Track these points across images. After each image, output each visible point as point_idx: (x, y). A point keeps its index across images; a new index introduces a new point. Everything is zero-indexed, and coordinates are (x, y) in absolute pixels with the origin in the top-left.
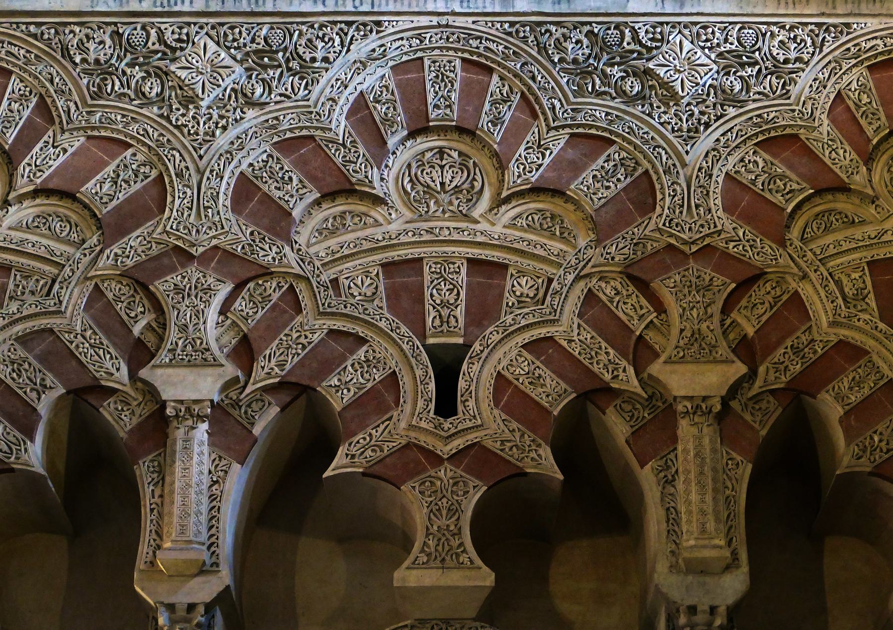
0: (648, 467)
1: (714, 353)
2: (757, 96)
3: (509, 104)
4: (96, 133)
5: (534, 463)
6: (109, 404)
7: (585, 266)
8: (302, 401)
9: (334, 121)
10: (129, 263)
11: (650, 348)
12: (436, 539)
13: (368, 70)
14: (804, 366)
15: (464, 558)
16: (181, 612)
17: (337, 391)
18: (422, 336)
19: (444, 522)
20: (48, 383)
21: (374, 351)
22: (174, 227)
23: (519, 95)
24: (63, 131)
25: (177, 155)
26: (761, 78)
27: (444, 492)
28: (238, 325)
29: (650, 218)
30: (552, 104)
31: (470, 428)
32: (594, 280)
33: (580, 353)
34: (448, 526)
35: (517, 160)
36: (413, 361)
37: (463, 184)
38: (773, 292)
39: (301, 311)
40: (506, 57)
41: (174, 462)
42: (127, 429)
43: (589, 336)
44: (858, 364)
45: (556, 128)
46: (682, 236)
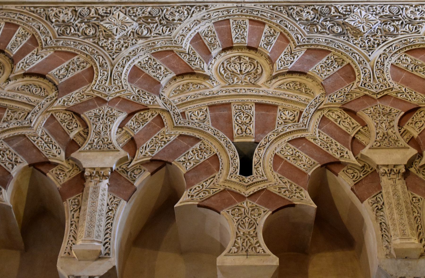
0: (366, 202)
1: (397, 144)
2: (403, 33)
3: (274, 37)
4: (59, 49)
5: (299, 199)
6: (52, 171)
7: (320, 105)
8: (163, 170)
10: (71, 104)
12: (242, 240)
13: (201, 24)
15: (259, 249)
18: (232, 138)
19: (246, 230)
20: (19, 160)
21: (204, 145)
22: (97, 88)
23: (279, 34)
24: (42, 49)
25: (101, 58)
26: (404, 26)
27: (246, 214)
28: (128, 133)
29: (353, 84)
31: (260, 181)
32: (326, 112)
33: (320, 145)
34: (249, 232)
35: (280, 60)
36: (227, 149)
37: (252, 70)
39: (164, 126)
40: (272, 18)
41: (87, 199)
42: (61, 184)
43: (325, 137)
45: (299, 46)
46: (372, 90)
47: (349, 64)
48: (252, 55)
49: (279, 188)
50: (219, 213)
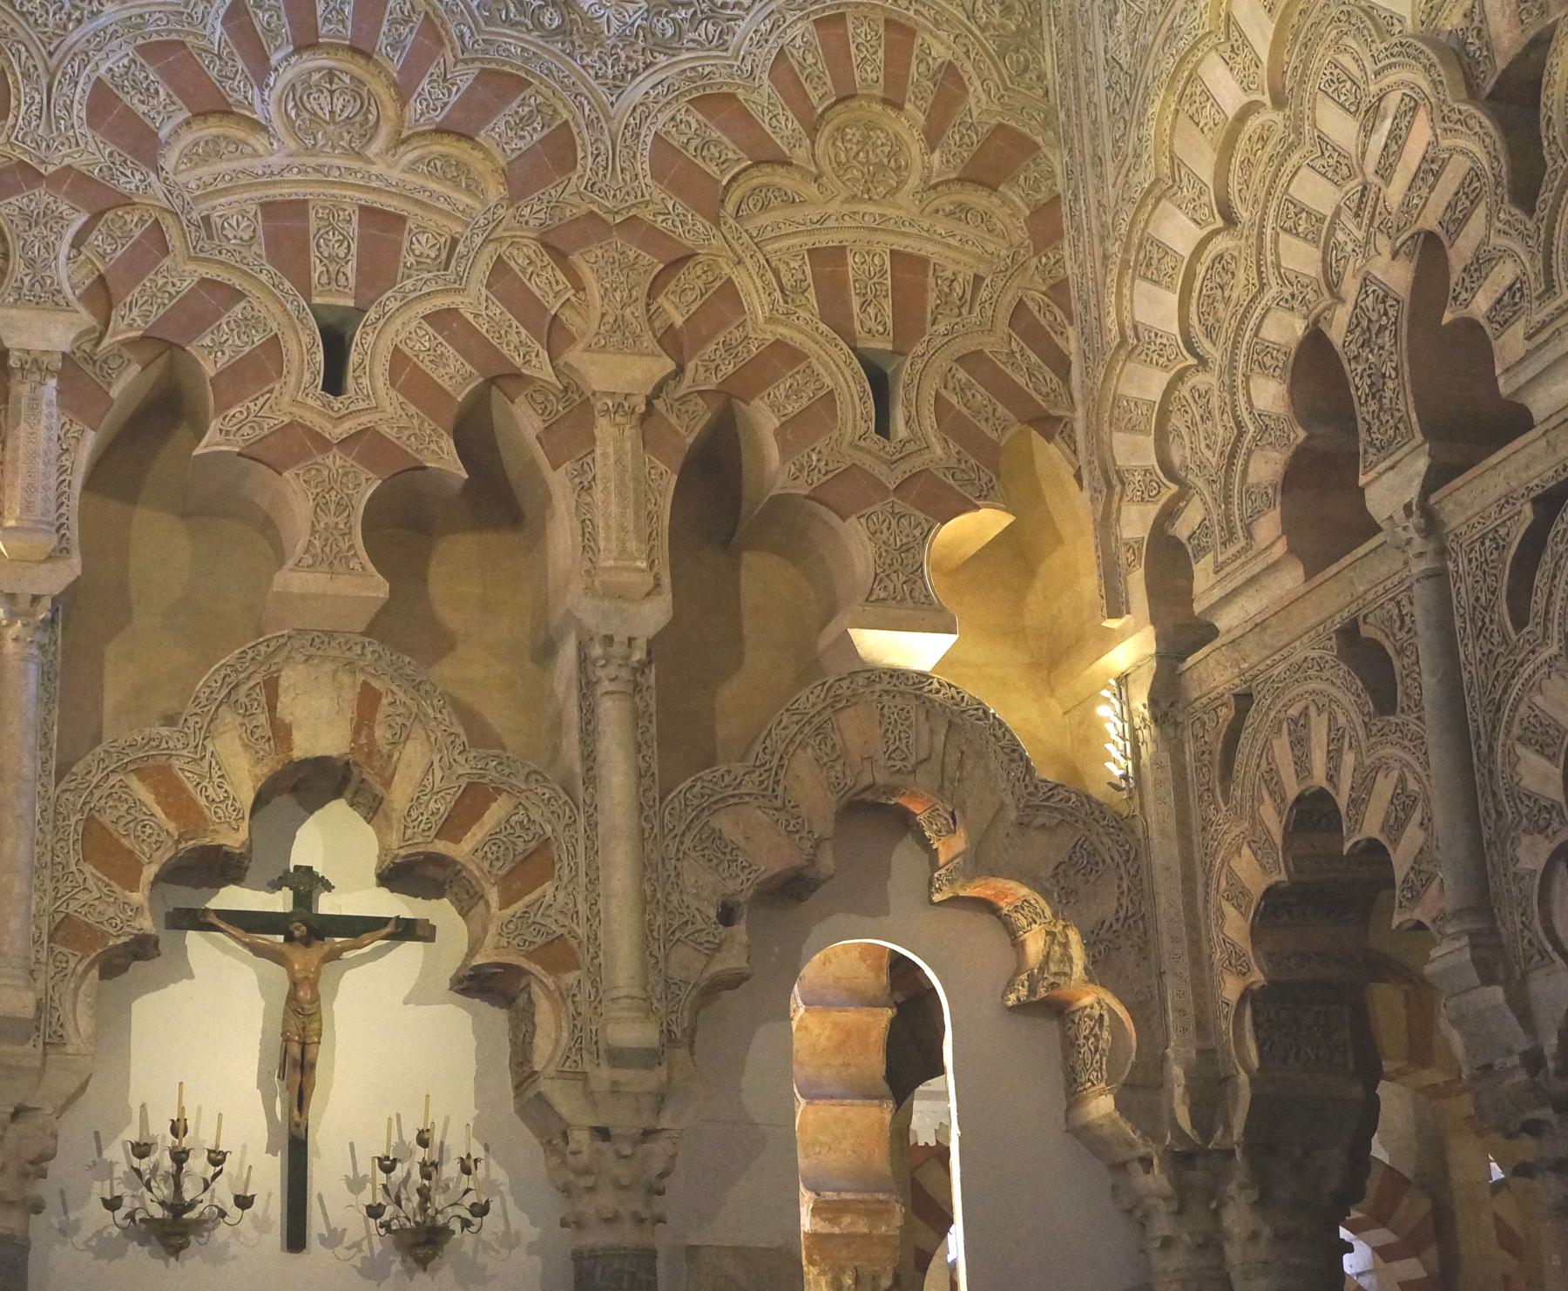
0: (562, 470)
2: (691, 45)
5: (436, 457)
9: (209, 26)
11: (563, 328)
16: (24, 604)
17: (210, 353)
18: (308, 296)
19: (331, 520)
21: (253, 309)
23: (422, 15)
25: (23, 49)
27: (333, 484)
28: (93, 263)
30: (461, 31)
35: (420, 94)
36: (299, 326)
38: (704, 277)
39: (168, 252)
41: (18, 424)
43: (498, 311)
44: (796, 370)
45: (465, 61)
47: (566, 122)
48: (357, 67)
50: (280, 474)
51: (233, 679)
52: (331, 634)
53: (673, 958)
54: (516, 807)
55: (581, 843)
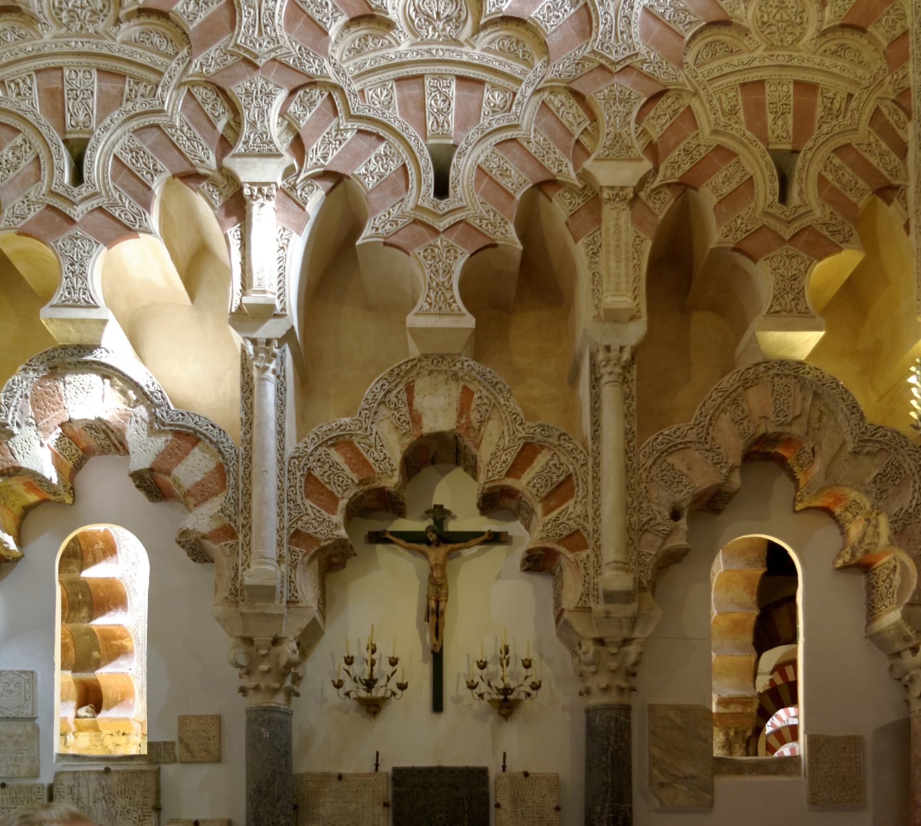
7: (539, 82)
8: (340, 188)
14: (692, 165)
29: (587, 43)
33: (535, 152)
37: (452, 13)
44: (728, 165)
49: (481, 220)
51: (386, 387)
52: (443, 357)
53: (643, 542)
54: (553, 456)
55: (590, 474)
